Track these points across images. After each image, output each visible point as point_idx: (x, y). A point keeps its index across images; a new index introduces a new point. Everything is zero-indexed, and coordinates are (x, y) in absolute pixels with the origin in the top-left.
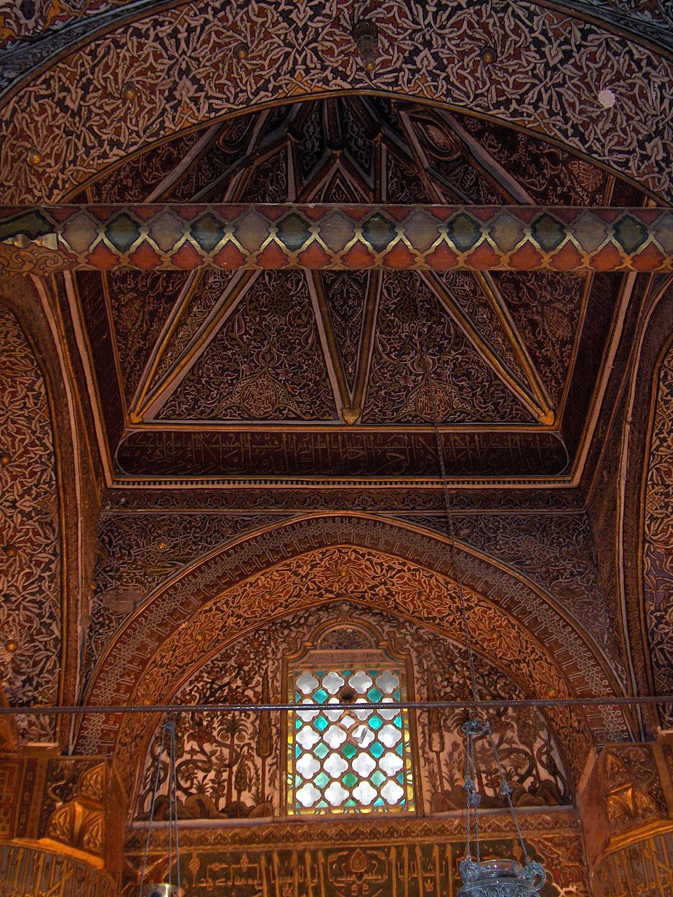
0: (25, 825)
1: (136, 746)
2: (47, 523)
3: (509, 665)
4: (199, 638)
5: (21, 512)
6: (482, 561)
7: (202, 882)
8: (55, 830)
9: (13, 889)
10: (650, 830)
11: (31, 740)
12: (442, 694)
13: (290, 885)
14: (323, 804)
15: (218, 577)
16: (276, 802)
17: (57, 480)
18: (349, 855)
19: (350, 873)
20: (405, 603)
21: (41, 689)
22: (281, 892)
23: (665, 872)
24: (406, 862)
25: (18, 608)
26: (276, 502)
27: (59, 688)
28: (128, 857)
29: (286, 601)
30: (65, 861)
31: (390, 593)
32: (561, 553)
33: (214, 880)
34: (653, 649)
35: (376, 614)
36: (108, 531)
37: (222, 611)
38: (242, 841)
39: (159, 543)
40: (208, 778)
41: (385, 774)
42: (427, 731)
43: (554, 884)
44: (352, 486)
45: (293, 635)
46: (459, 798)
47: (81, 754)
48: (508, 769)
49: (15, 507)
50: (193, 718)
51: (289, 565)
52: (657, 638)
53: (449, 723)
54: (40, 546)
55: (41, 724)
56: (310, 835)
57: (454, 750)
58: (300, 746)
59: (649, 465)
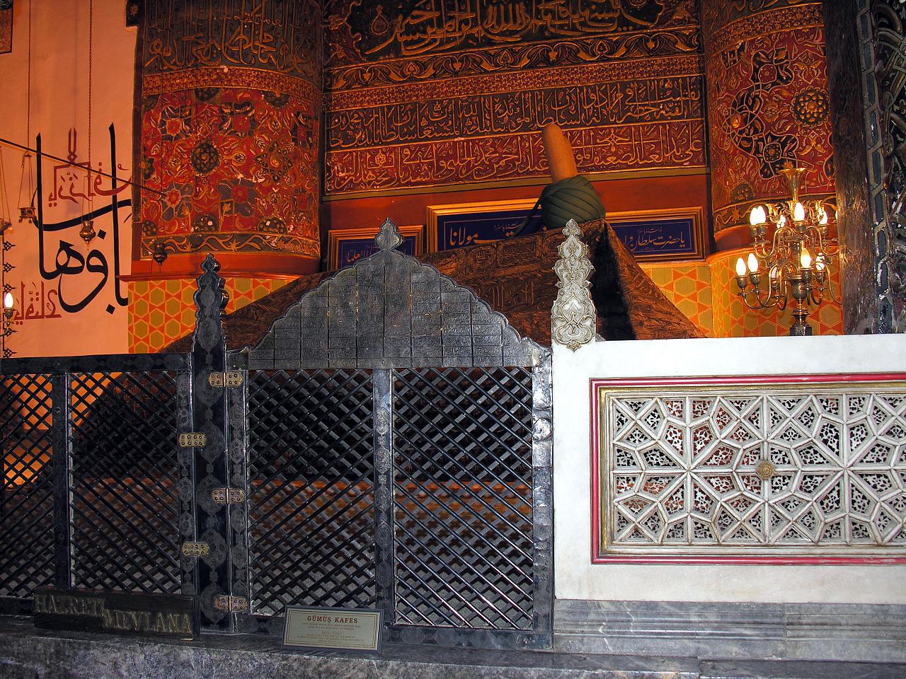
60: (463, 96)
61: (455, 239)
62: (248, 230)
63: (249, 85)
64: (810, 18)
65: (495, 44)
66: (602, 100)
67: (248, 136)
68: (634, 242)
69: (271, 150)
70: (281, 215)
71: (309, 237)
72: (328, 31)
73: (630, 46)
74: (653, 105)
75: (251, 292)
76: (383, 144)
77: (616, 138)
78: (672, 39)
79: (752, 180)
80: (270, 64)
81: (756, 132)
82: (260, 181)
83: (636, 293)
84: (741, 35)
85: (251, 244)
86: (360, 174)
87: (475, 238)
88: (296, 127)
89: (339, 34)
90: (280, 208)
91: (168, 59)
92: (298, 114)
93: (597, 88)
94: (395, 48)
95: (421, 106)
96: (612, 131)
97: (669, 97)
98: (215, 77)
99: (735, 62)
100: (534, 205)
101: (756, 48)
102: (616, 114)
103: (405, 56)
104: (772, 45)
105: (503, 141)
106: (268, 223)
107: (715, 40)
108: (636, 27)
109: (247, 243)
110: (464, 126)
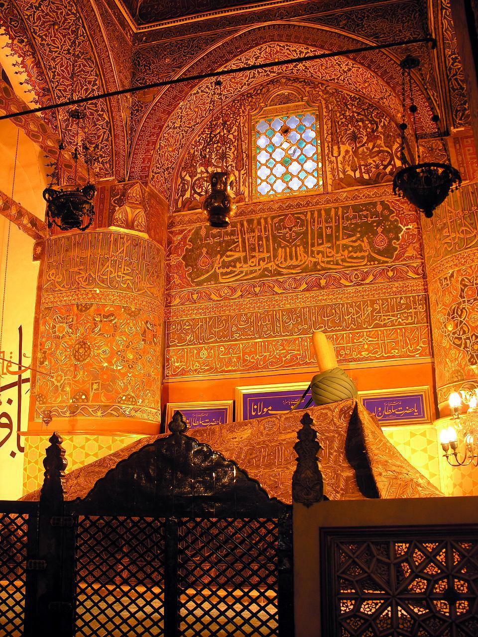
6: (353, 39)
7: (207, 240)
11: (101, 177)
12: (340, 123)
13: (253, 237)
14: (272, 192)
16: (246, 194)
18: (285, 218)
20: (316, 72)
21: (103, 150)
22: (248, 241)
23: (451, 212)
24: (316, 219)
26: (230, 23)
29: (248, 81)
30: (126, 237)
32: (403, 27)
34: (450, 79)
36: (137, 58)
37: (207, 93)
39: (165, 59)
43: (400, 225)
45: (254, 101)
46: (349, 182)
49: (69, 53)
50: (201, 155)
51: (240, 60)
53: (344, 139)
56: (264, 210)
57: (346, 154)
61: (255, 410)
63: (113, 302)
65: (283, 275)
66: (357, 312)
68: (381, 412)
69: (127, 347)
70: (133, 392)
71: (153, 408)
72: (169, 265)
74: (393, 316)
75: (110, 446)
77: (367, 339)
78: (405, 270)
80: (128, 287)
81: (464, 333)
82: (119, 368)
83: (376, 452)
84: (451, 267)
85: (112, 412)
86: (190, 364)
87: (269, 410)
88: (145, 331)
89: (177, 267)
90: (133, 387)
92: (147, 322)
93: (354, 304)
94: (215, 277)
95: (232, 317)
96: (365, 334)
97: (403, 310)
98: (90, 296)
99: (447, 285)
100: (307, 387)
101: (462, 275)
103: (221, 283)
104: (473, 273)
106: (124, 398)
107: (434, 270)
108: (379, 261)
109: (109, 411)
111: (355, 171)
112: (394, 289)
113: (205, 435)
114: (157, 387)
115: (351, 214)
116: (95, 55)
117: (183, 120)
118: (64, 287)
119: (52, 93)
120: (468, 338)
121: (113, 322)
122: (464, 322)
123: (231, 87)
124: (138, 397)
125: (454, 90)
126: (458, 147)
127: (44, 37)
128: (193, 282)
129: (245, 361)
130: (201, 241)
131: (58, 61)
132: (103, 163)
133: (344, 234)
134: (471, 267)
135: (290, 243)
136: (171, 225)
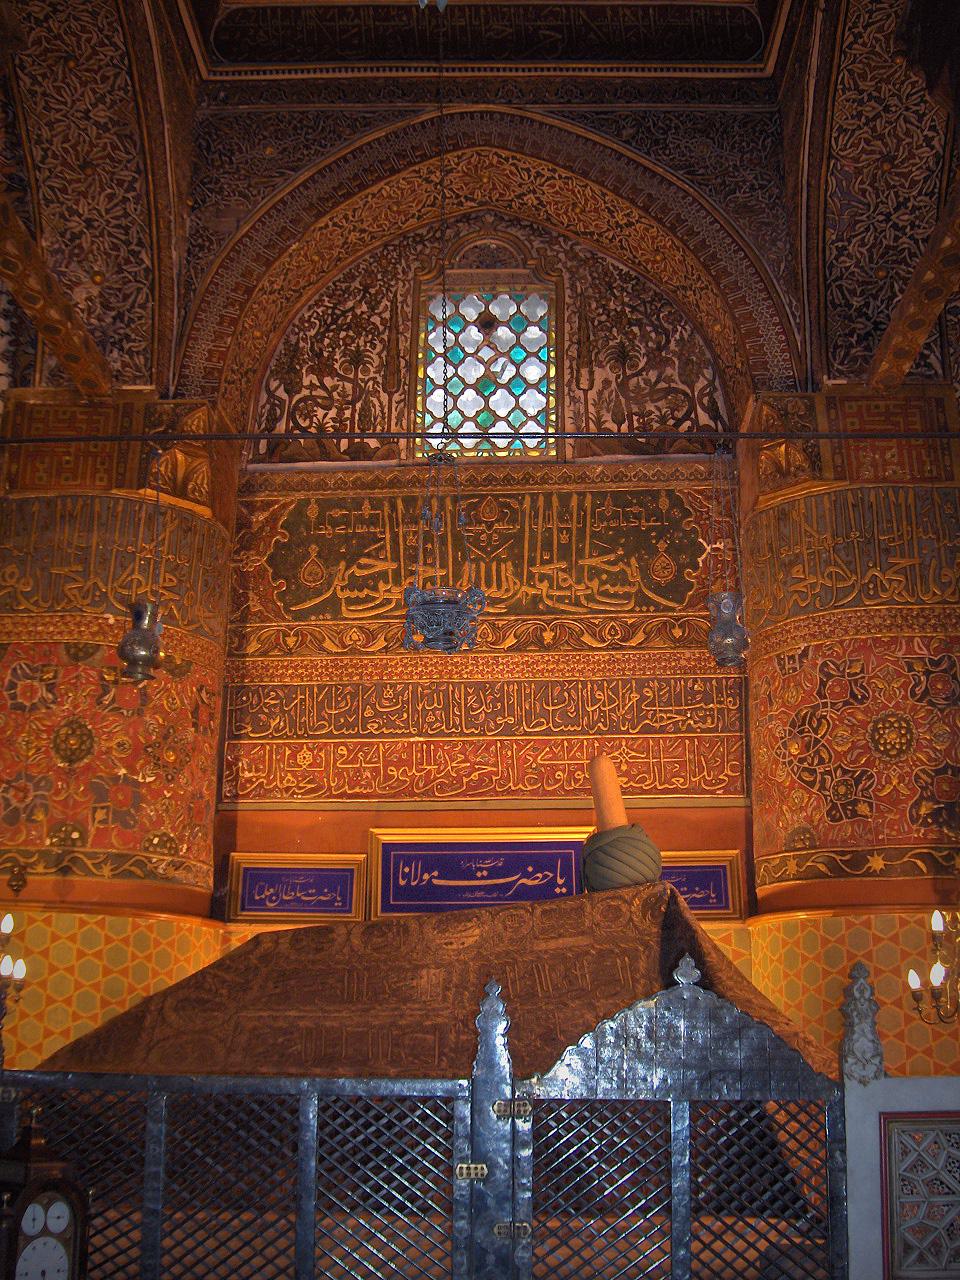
0: (123, 475)
1: (248, 381)
2: (126, 136)
3: (675, 292)
4: (316, 258)
5: (96, 124)
6: (646, 169)
7: (321, 529)
8: (156, 480)
9: (114, 542)
10: (801, 490)
11: (125, 382)
12: (596, 323)
13: (415, 533)
15: (334, 189)
17: (133, 86)
19: (480, 522)
22: (405, 540)
23: (811, 536)
24: (541, 511)
25: (102, 235)
27: (153, 324)
28: (241, 503)
29: (419, 211)
30: (169, 512)
31: (541, 203)
32: (742, 160)
33: (333, 527)
35: (525, 227)
37: (341, 227)
38: (364, 486)
39: (265, 148)
40: (329, 416)
41: (525, 413)
42: (575, 367)
44: (496, 74)
47: (183, 395)
48: (664, 411)
49: (88, 118)
52: (836, 273)
53: (601, 357)
54: (120, 162)
55: (136, 364)
57: (604, 388)
58: (432, 380)
59: (839, 66)
60: (425, 681)
62: (130, 849)
64: (892, 624)
67: (136, 717)
70: (174, 829)
71: (203, 862)
73: (651, 631)
74: (678, 713)
76: (309, 737)
79: (816, 823)
82: (149, 780)
83: (730, 983)
84: (803, 638)
85: (133, 868)
87: (434, 877)
91: (27, 596)
94: (332, 606)
95: (366, 690)
96: (624, 743)
97: (699, 702)
98: (96, 629)
99: (795, 670)
101: (824, 656)
102: (629, 721)
103: (346, 619)
104: (845, 651)
105: (477, 747)
106: (156, 841)
107: (767, 638)
108: (658, 607)
109: (126, 866)
110: (424, 722)
111: (619, 425)
112: (683, 663)
113: (390, 934)
114: (210, 817)
115: (609, 508)
116: (142, 132)
117: (289, 277)
118: (36, 603)
119: (34, 192)
120: (829, 773)
121: (140, 686)
122: (823, 741)
123: (387, 219)
124: (181, 840)
125: (835, 306)
126: (833, 417)
127: (40, 79)
128: (288, 611)
129: (388, 777)
130: (308, 529)
131: (59, 129)
132: (130, 352)
133: (593, 546)
134: (841, 642)
135: (488, 554)
136: (248, 488)
